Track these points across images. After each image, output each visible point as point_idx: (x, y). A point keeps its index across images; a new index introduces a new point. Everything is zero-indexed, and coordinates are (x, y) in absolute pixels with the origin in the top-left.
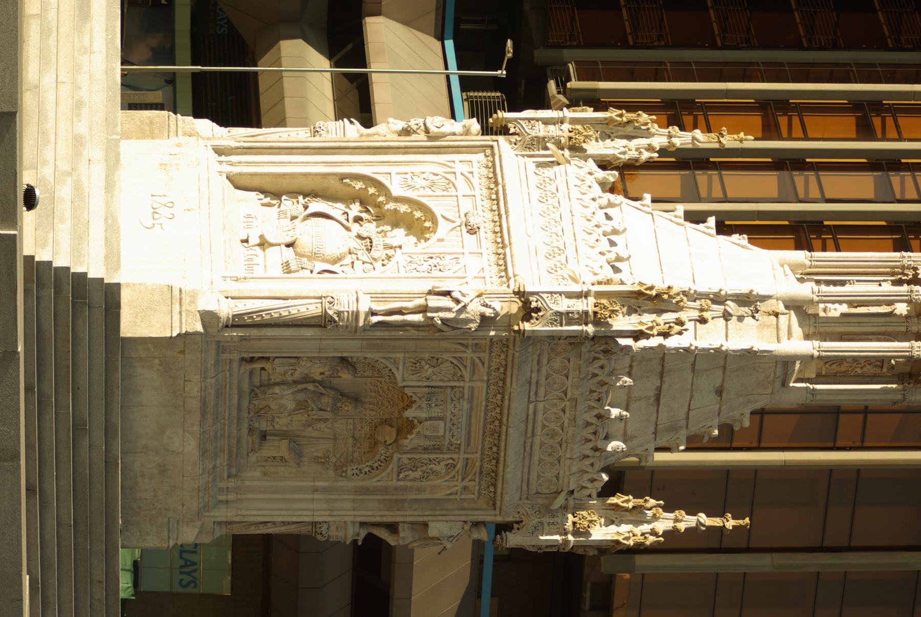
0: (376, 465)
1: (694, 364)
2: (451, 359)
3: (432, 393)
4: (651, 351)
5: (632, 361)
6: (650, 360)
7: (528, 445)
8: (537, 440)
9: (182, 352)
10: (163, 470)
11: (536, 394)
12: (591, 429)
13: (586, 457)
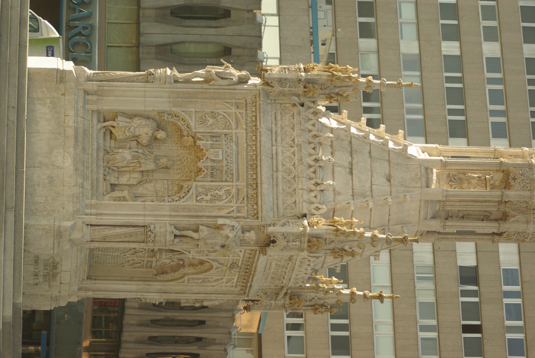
0: (183, 195)
1: (370, 153)
2: (223, 113)
3: (215, 136)
4: (343, 132)
6: (342, 140)
7: (275, 177)
8: (280, 174)
9: (64, 94)
10: (51, 180)
11: (276, 140)
12: (312, 170)
13: (311, 191)
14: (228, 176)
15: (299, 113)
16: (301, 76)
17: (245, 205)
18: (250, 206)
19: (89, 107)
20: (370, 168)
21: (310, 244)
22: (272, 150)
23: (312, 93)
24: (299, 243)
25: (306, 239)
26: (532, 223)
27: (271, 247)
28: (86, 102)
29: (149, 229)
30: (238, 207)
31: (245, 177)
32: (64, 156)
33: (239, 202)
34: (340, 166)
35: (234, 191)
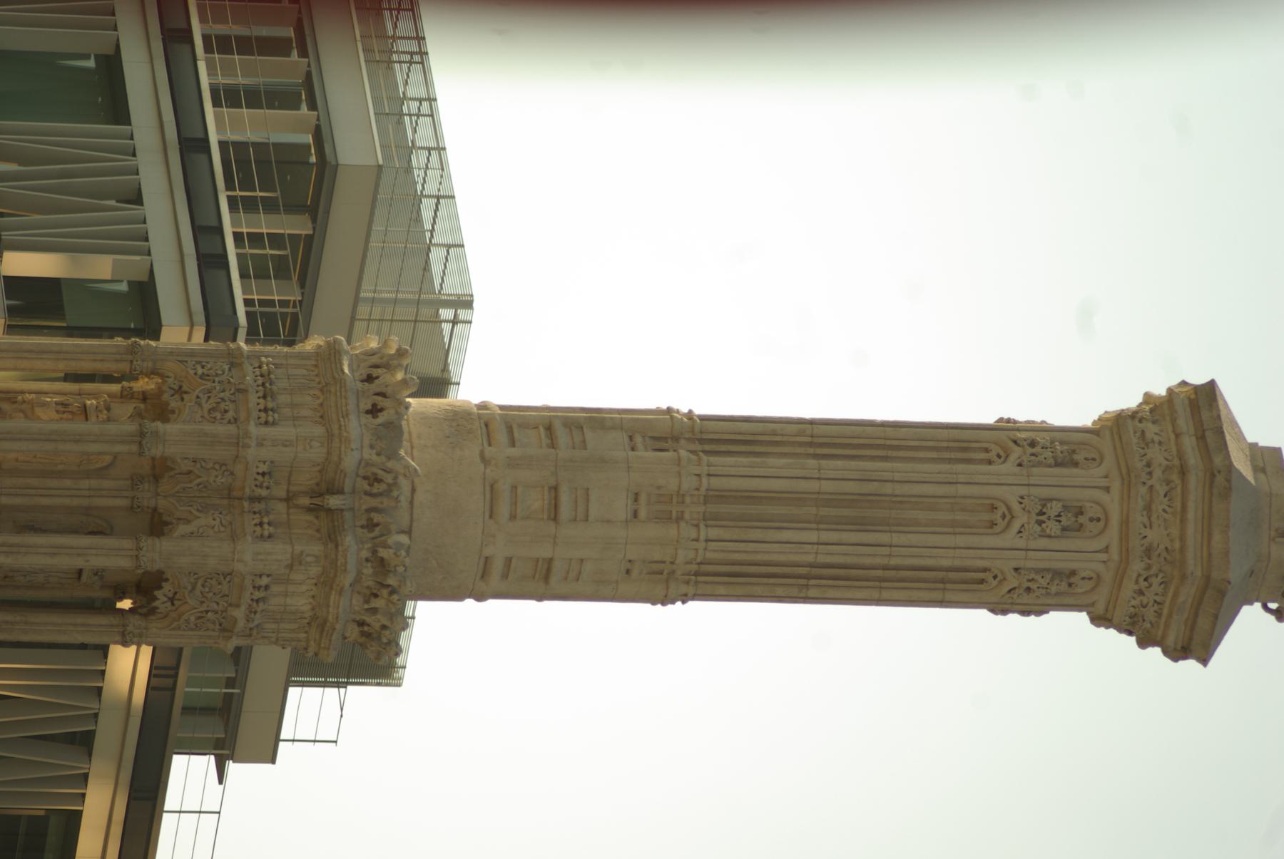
26: (249, 538)
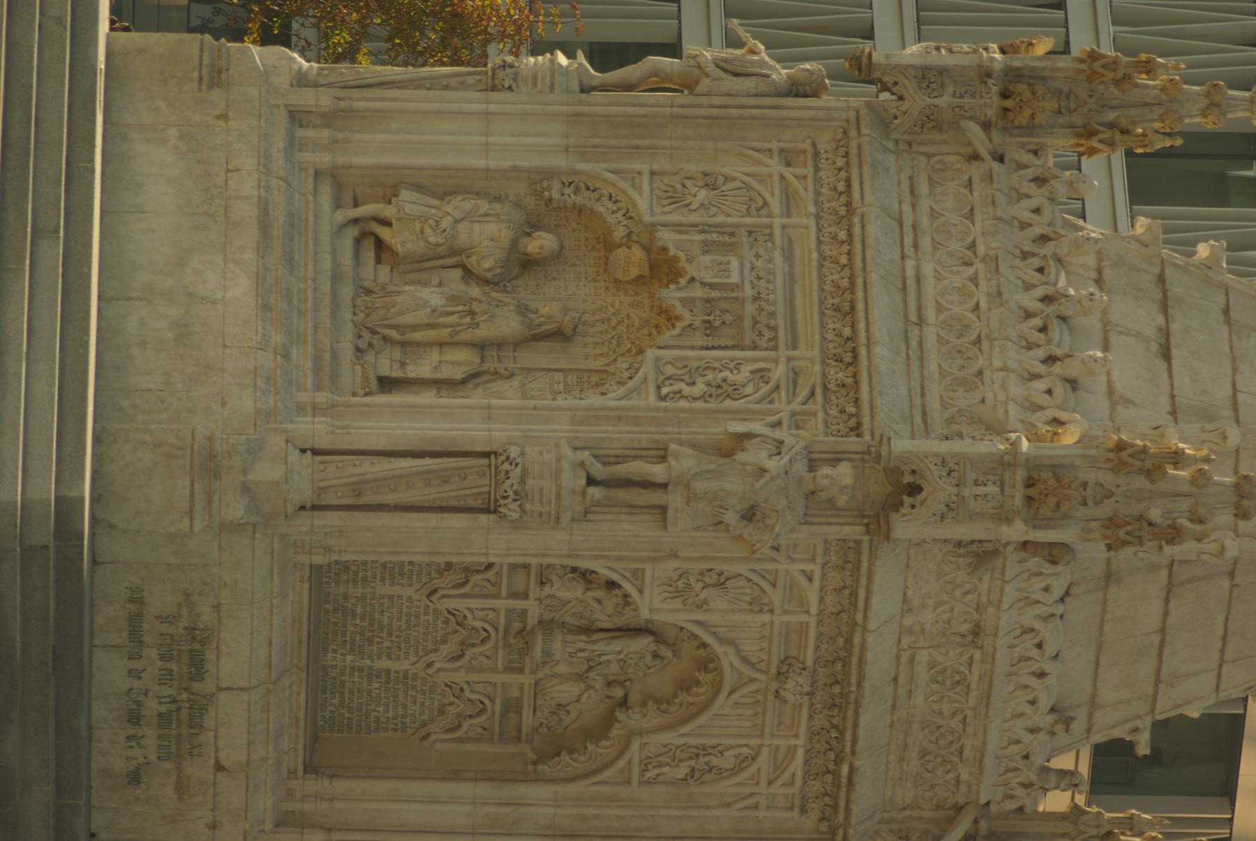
1: (1226, 311)
5: (1100, 260)
8: (931, 333)
10: (183, 331)
11: (916, 245)
13: (1035, 376)
14: (760, 334)
15: (989, 177)
16: (993, 59)
17: (819, 407)
18: (834, 412)
19: (307, 157)
20: (1227, 349)
21: (1032, 492)
22: (904, 270)
23: (1027, 112)
24: (992, 489)
25: (1020, 474)
27: (906, 510)
28: (293, 145)
29: (503, 458)
30: (794, 414)
31: (817, 337)
32: (225, 272)
33: (799, 399)
34: (1128, 334)
35: (779, 372)
